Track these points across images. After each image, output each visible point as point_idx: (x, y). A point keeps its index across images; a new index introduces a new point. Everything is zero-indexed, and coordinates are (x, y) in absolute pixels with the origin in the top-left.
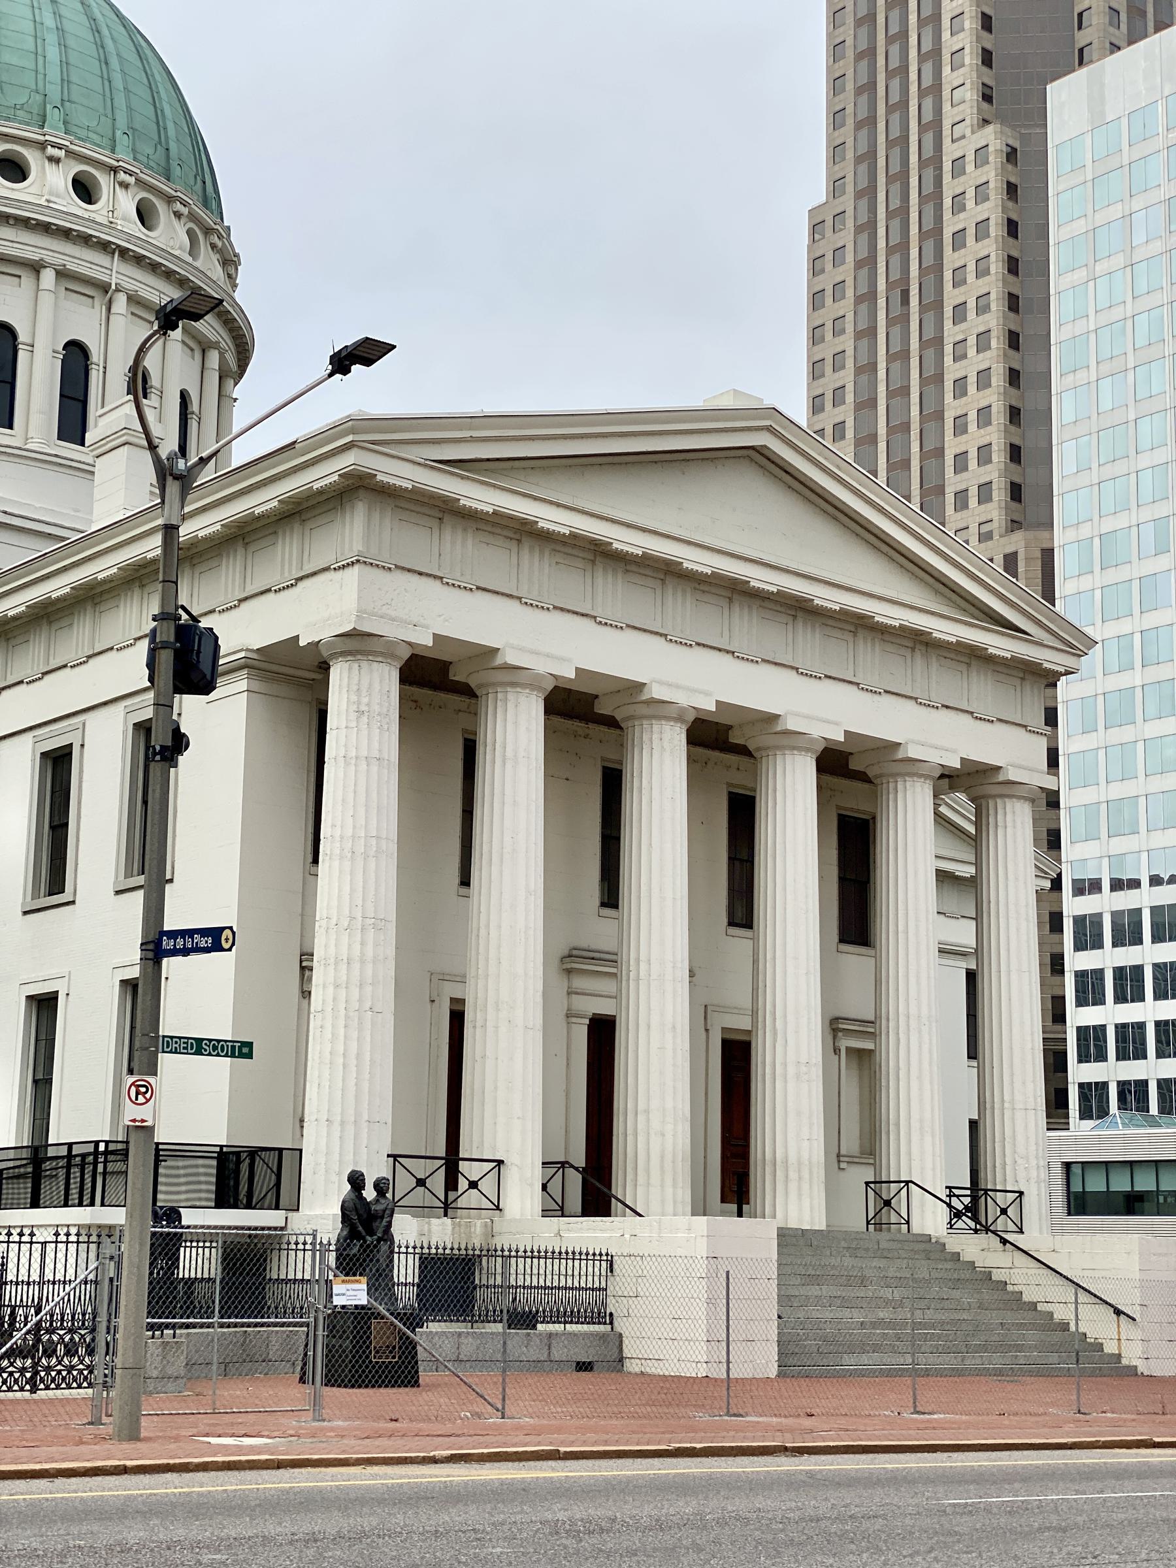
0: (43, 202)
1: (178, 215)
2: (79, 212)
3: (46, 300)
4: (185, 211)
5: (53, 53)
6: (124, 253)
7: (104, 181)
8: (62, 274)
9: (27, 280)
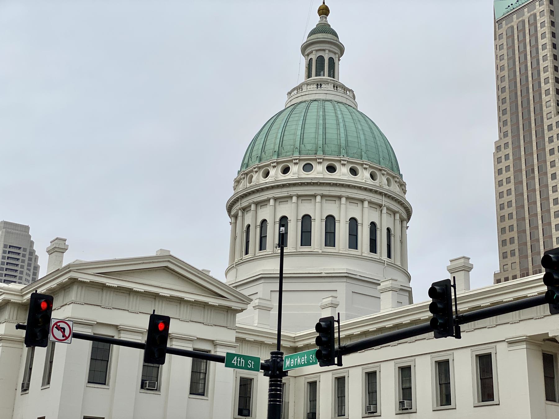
0: (363, 181)
1: (396, 182)
2: (372, 183)
3: (366, 211)
4: (398, 180)
5: (362, 137)
6: (386, 195)
7: (378, 173)
8: (370, 202)
9: (360, 205)
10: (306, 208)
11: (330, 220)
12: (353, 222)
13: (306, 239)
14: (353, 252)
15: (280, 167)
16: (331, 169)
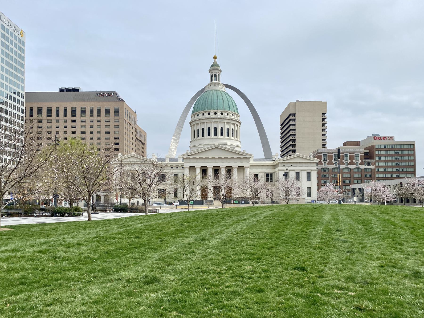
7: (229, 113)
10: (209, 126)
11: (215, 129)
12: (222, 129)
13: (209, 134)
14: (222, 137)
15: (202, 113)
16: (215, 113)
